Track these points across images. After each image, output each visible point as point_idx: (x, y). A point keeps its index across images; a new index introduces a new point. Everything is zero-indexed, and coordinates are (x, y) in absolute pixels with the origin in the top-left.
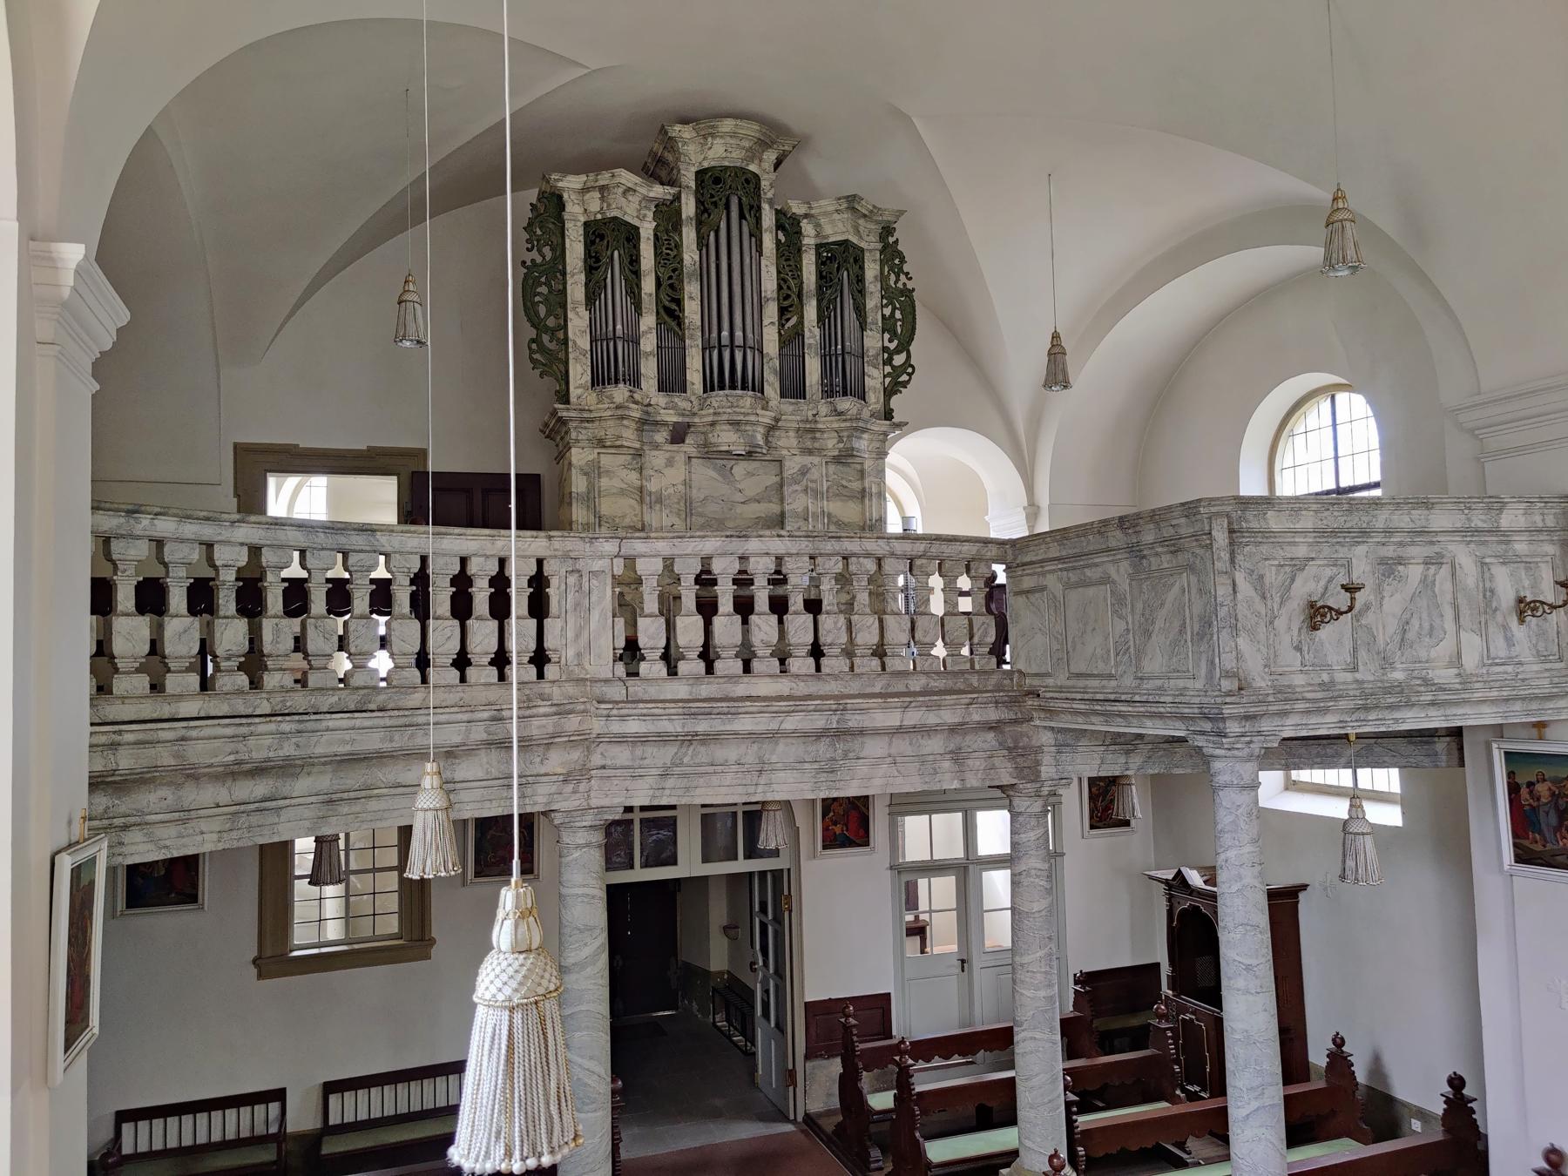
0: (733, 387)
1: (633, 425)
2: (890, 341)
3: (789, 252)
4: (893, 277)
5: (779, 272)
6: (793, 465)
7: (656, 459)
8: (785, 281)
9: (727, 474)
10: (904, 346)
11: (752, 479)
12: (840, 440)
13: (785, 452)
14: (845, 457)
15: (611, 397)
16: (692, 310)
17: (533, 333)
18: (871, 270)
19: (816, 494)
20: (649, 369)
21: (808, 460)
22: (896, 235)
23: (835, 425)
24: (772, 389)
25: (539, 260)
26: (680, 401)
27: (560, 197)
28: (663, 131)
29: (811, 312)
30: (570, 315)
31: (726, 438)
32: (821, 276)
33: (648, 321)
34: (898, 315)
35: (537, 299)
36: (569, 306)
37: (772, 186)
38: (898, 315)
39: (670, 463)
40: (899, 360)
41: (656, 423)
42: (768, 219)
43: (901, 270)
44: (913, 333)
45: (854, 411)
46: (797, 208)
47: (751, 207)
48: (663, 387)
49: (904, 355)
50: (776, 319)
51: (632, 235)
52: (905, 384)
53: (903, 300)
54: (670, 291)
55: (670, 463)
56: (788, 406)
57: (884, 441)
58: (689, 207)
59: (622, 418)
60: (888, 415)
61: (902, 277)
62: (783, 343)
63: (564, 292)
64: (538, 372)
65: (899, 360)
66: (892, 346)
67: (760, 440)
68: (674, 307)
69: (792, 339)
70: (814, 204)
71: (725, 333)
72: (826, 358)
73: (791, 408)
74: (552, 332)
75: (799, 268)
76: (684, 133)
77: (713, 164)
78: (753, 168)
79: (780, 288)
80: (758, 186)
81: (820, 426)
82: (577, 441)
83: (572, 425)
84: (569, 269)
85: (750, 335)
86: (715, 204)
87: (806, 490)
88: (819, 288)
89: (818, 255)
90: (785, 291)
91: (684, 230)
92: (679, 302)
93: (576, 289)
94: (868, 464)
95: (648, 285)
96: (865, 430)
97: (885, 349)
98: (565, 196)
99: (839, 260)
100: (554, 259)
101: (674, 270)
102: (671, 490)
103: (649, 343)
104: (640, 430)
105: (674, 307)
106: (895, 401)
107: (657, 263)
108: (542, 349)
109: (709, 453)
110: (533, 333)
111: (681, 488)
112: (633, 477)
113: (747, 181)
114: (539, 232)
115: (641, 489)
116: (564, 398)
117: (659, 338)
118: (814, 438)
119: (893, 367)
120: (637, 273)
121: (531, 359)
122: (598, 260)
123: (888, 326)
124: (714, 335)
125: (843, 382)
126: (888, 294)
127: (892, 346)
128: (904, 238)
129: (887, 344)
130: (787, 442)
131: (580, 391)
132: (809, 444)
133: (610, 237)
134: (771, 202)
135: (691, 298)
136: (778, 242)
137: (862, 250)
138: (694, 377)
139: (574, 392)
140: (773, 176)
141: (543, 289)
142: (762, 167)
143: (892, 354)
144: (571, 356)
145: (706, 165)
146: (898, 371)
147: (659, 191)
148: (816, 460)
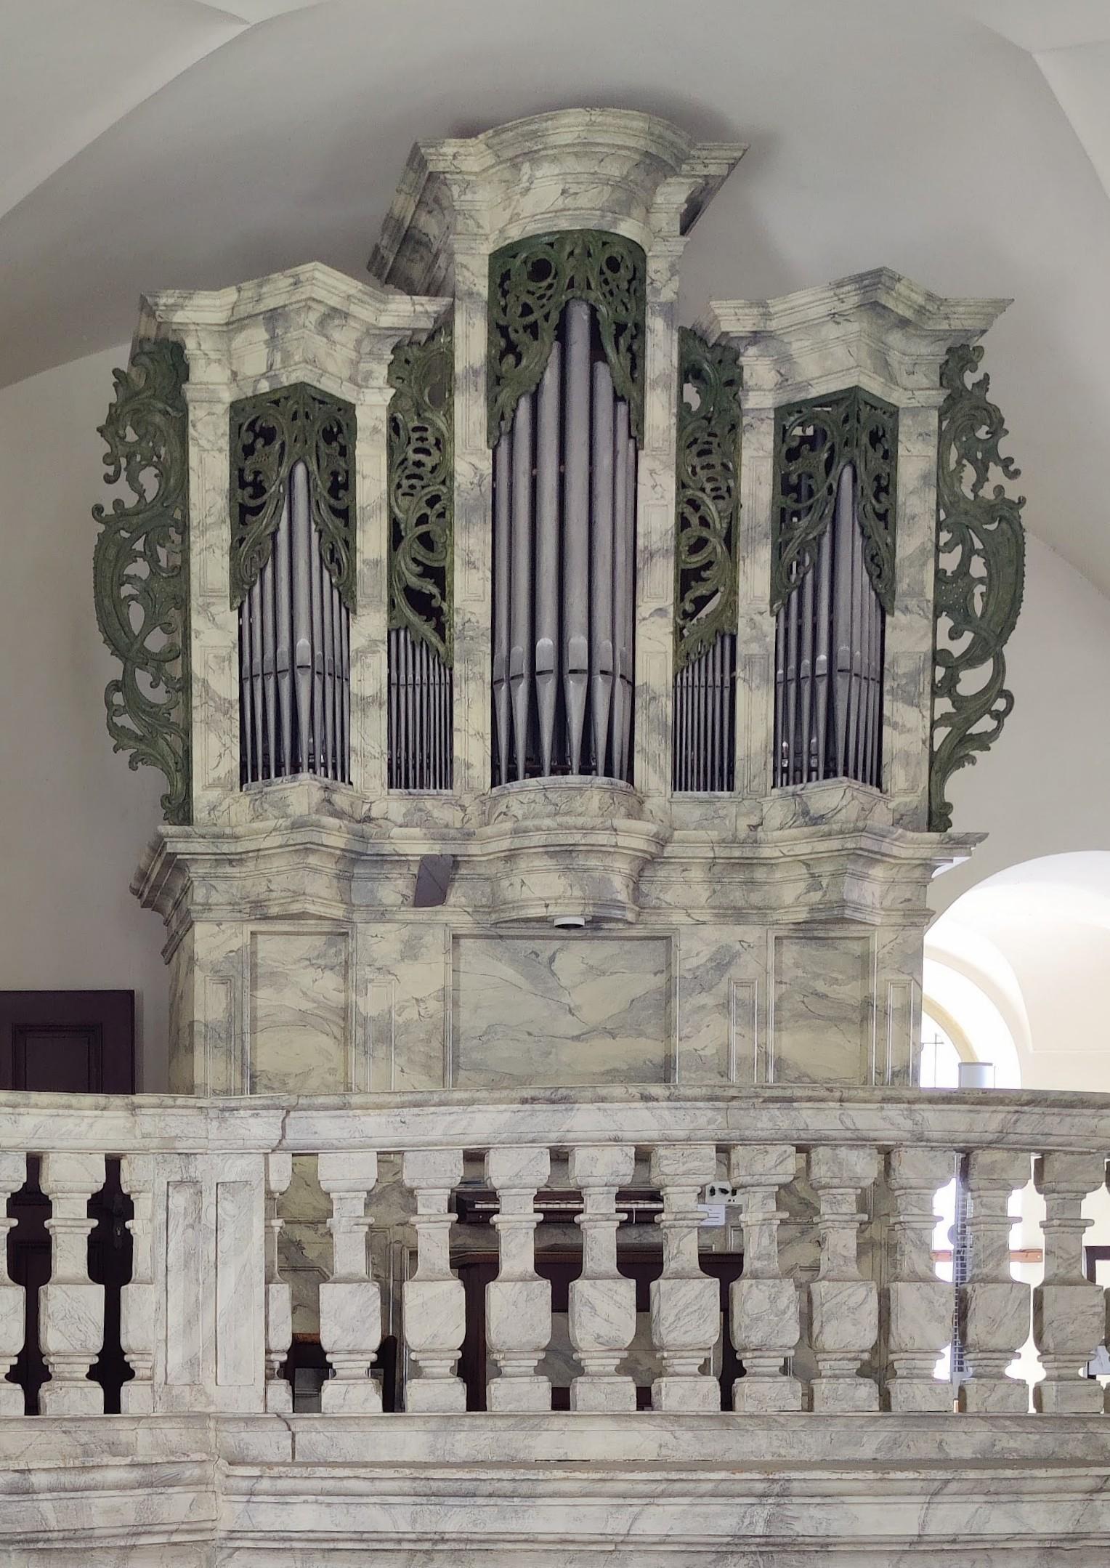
0: (561, 767)
1: (330, 867)
2: (954, 634)
3: (708, 440)
4: (970, 474)
5: (682, 486)
6: (695, 949)
7: (381, 941)
8: (694, 504)
9: (540, 973)
10: (990, 644)
11: (598, 982)
12: (814, 882)
13: (678, 918)
14: (825, 925)
15: (282, 805)
16: (470, 593)
17: (114, 668)
18: (915, 459)
19: (751, 1014)
20: (369, 737)
21: (731, 934)
22: (984, 366)
23: (803, 848)
24: (653, 770)
25: (131, 500)
26: (435, 804)
27: (178, 348)
28: (417, 160)
29: (755, 577)
30: (197, 622)
31: (543, 889)
32: (786, 486)
33: (370, 625)
34: (978, 568)
35: (126, 590)
36: (195, 602)
37: (673, 270)
38: (978, 568)
39: (411, 950)
40: (973, 681)
41: (382, 860)
43: (991, 453)
44: (1017, 600)
45: (850, 813)
46: (732, 319)
47: (620, 328)
48: (399, 776)
49: (990, 663)
50: (668, 600)
51: (336, 426)
52: (984, 741)
53: (993, 537)
54: (421, 553)
55: (411, 950)
56: (691, 807)
57: (923, 883)
58: (471, 343)
59: (307, 849)
60: (937, 817)
61: (995, 473)
62: (684, 661)
63: (182, 571)
64: (125, 755)
65: (973, 681)
66: (957, 648)
67: (619, 888)
68: (429, 587)
69: (707, 646)
70: (776, 306)
71: (546, 642)
72: (791, 689)
73: (697, 813)
74: (157, 663)
75: (731, 470)
76: (469, 158)
77: (533, 228)
78: (628, 229)
79: (683, 523)
80: (638, 276)
81: (766, 852)
82: (207, 907)
83: (196, 871)
84: (195, 516)
85: (603, 641)
86: (533, 330)
87: (725, 1006)
88: (783, 517)
89: (782, 433)
90: (696, 530)
92: (439, 576)
93: (210, 563)
94: (881, 940)
95: (371, 541)
96: (874, 858)
97: (938, 657)
98: (190, 345)
99: (837, 444)
100: (162, 496)
101: (433, 501)
102: (411, 1013)
103: (369, 677)
104: (345, 878)
105: (429, 587)
106: (957, 786)
107: (394, 486)
108: (136, 705)
109: (503, 927)
110: (114, 668)
111: (434, 1006)
112: (328, 984)
113: (613, 264)
114: (131, 436)
115: (345, 1012)
116: (179, 808)
117: (394, 662)
118: (751, 883)
119: (958, 701)
120: (345, 515)
121: (114, 729)
122: (259, 489)
123: (950, 597)
124: (521, 647)
125: (829, 744)
126: (956, 519)
127: (957, 648)
128: (1005, 379)
129: (944, 642)
130: (684, 892)
131: (214, 795)
132: (737, 896)
133: (290, 434)
134: (669, 311)
135: (470, 564)
136: (683, 410)
137: (893, 412)
138: (471, 748)
139: (202, 796)
140: (678, 245)
141: (140, 568)
142: (652, 228)
143: (954, 666)
144: (197, 716)
145: (515, 234)
146: (968, 709)
147: (404, 311)
148: (752, 933)
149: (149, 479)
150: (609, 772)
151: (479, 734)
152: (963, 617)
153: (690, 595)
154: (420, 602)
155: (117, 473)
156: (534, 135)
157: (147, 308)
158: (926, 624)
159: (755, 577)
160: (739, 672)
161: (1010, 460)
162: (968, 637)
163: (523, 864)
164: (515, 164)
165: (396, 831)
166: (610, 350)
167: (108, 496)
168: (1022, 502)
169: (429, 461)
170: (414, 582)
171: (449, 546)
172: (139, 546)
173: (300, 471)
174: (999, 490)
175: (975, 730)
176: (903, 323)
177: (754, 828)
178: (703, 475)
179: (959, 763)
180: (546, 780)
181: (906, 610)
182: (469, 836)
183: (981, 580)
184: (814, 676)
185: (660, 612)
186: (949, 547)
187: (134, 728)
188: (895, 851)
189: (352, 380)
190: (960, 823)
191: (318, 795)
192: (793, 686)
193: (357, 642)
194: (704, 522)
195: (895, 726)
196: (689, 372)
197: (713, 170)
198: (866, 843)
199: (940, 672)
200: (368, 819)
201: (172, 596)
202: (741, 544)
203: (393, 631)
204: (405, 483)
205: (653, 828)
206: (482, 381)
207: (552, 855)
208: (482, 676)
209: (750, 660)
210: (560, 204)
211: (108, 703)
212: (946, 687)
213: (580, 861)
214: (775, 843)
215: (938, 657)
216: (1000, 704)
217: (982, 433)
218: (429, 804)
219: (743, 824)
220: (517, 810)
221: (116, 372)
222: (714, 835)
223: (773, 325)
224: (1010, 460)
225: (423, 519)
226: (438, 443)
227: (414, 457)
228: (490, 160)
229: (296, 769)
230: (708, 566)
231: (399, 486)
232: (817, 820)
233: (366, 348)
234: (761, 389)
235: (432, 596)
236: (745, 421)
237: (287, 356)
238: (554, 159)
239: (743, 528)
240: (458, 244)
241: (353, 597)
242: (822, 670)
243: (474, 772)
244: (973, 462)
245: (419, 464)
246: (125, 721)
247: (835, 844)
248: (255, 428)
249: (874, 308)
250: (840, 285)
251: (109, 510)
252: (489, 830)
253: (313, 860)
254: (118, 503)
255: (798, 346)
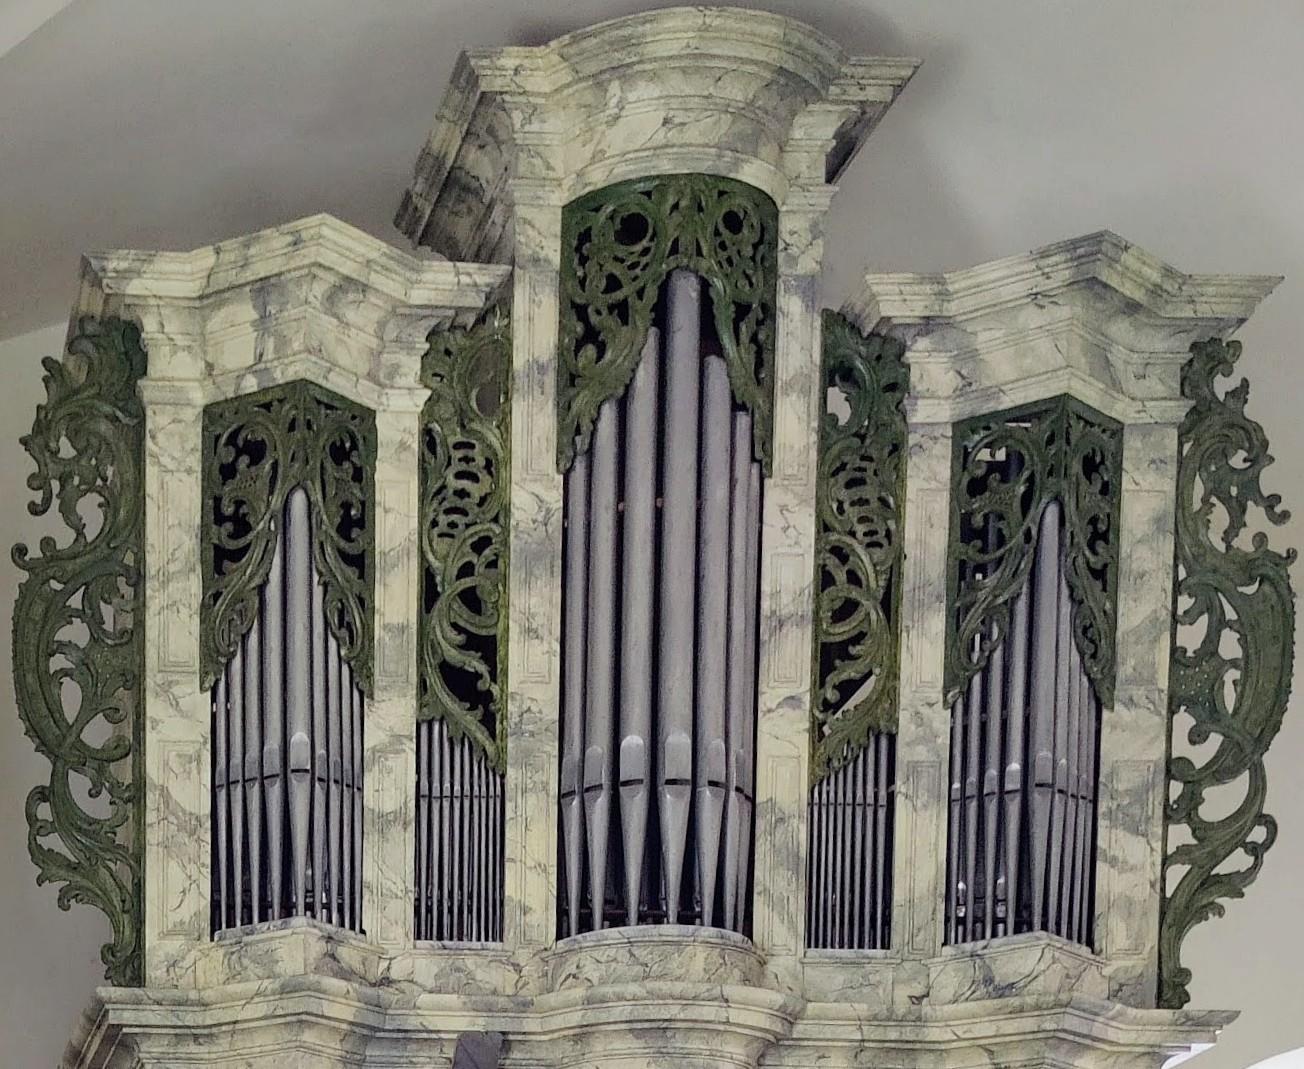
0: (653, 913)
2: (1196, 737)
3: (861, 464)
4: (1220, 516)
10: (1246, 748)
15: (268, 961)
16: (530, 672)
17: (40, 770)
18: (1145, 495)
20: (388, 868)
22: (1241, 369)
23: (985, 1029)
24: (779, 918)
25: (65, 538)
27: (133, 330)
28: (464, 75)
29: (923, 653)
30: (154, 707)
32: (966, 530)
33: (392, 714)
34: (1230, 646)
35: (58, 662)
36: (151, 682)
37: (816, 232)
38: (1230, 646)
40: (1221, 801)
42: (798, 345)
45: (1050, 983)
46: (894, 299)
51: (348, 441)
52: (1235, 885)
58: (536, 329)
60: (1170, 989)
61: (1255, 516)
62: (825, 768)
64: (53, 889)
65: (1221, 801)
68: (474, 663)
70: (957, 282)
71: (634, 741)
73: (840, 978)
76: (534, 73)
77: (623, 171)
78: (754, 173)
80: (767, 238)
81: (933, 1033)
85: (713, 741)
86: (622, 311)
88: (962, 573)
89: (963, 457)
90: (842, 589)
91: (519, 408)
93: (174, 625)
95: (396, 599)
97: (1173, 767)
98: (150, 326)
99: (1038, 471)
103: (390, 785)
105: (474, 663)
106: (1198, 947)
108: (69, 820)
110: (40, 770)
113: (733, 222)
114: (67, 450)
117: (424, 767)
119: (1200, 829)
121: (38, 854)
123: (1191, 686)
124: (600, 747)
125: (1017, 884)
126: (1201, 578)
129: (1181, 748)
134: (809, 288)
135: (530, 632)
137: (1117, 430)
138: (530, 887)
140: (822, 196)
141: (76, 633)
142: (787, 171)
144: (153, 836)
145: (598, 178)
146: (1213, 840)
147: (444, 283)
149: (90, 509)
150: (718, 921)
151: (541, 867)
152: (1209, 714)
153: (833, 679)
154: (461, 683)
155: (47, 501)
156: (626, 43)
157: (91, 275)
158: (1158, 722)
159: (923, 653)
160: (900, 786)
161: (1276, 499)
162: (1215, 741)
163: (598, 1046)
164: (599, 82)
165: (425, 999)
166: (727, 340)
167: (33, 532)
168: (1291, 555)
169: (476, 490)
170: (454, 656)
171: (501, 607)
172: (75, 602)
173: (299, 501)
174: (1261, 539)
175: (1222, 869)
176: (1132, 307)
177: (917, 1000)
178: (852, 513)
179: (1201, 915)
180: (632, 930)
181: (1131, 703)
182: (525, 1006)
183: (1234, 663)
184: (1002, 792)
185: (792, 701)
186: (1191, 617)
187: (65, 852)
188: (1111, 1035)
189: (371, 376)
190: (1201, 997)
191: (318, 948)
192: (973, 806)
193: (373, 738)
194: (853, 578)
195: (1113, 862)
196: (836, 372)
197: (871, 94)
198: (1071, 1022)
199: (1176, 789)
200: (386, 981)
201: (120, 672)
202: (905, 609)
203: (424, 723)
204: (443, 520)
205: (778, 999)
206: (550, 380)
207: (639, 1034)
208: (545, 787)
209: (915, 768)
210: (660, 138)
211: (31, 818)
212: (1183, 810)
213: (678, 1042)
214: (946, 1022)
215: (1173, 767)
216: (1258, 834)
217: (1238, 460)
218: (470, 962)
219: (902, 995)
220: (591, 971)
221: (47, 362)
222: (862, 1009)
223: (952, 308)
224: (1276, 499)
225: (467, 570)
226: (488, 465)
227: (455, 484)
228: (566, 77)
229: (288, 910)
230: (858, 639)
231: (435, 524)
232: (1004, 990)
233: (391, 333)
234: (935, 398)
235: (478, 676)
236: (912, 439)
237: (282, 342)
238: (654, 77)
239: (906, 587)
240: (520, 192)
241: (370, 676)
242: (1013, 783)
243: (533, 919)
244: (1226, 500)
245: (462, 494)
246: (53, 842)
247: (1028, 1023)
248: (238, 441)
249: (1093, 286)
250: (1044, 254)
251: (34, 552)
252: (552, 999)
253: (309, 1037)
254: (47, 543)
255: (985, 338)
